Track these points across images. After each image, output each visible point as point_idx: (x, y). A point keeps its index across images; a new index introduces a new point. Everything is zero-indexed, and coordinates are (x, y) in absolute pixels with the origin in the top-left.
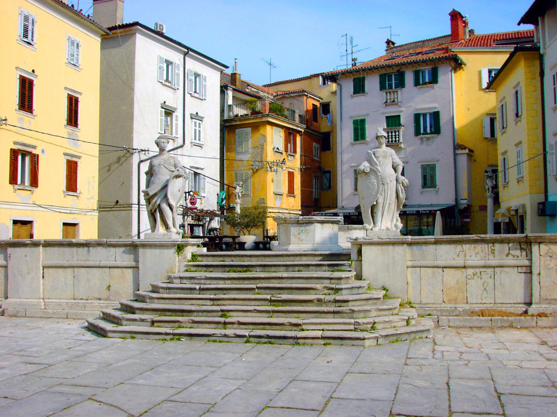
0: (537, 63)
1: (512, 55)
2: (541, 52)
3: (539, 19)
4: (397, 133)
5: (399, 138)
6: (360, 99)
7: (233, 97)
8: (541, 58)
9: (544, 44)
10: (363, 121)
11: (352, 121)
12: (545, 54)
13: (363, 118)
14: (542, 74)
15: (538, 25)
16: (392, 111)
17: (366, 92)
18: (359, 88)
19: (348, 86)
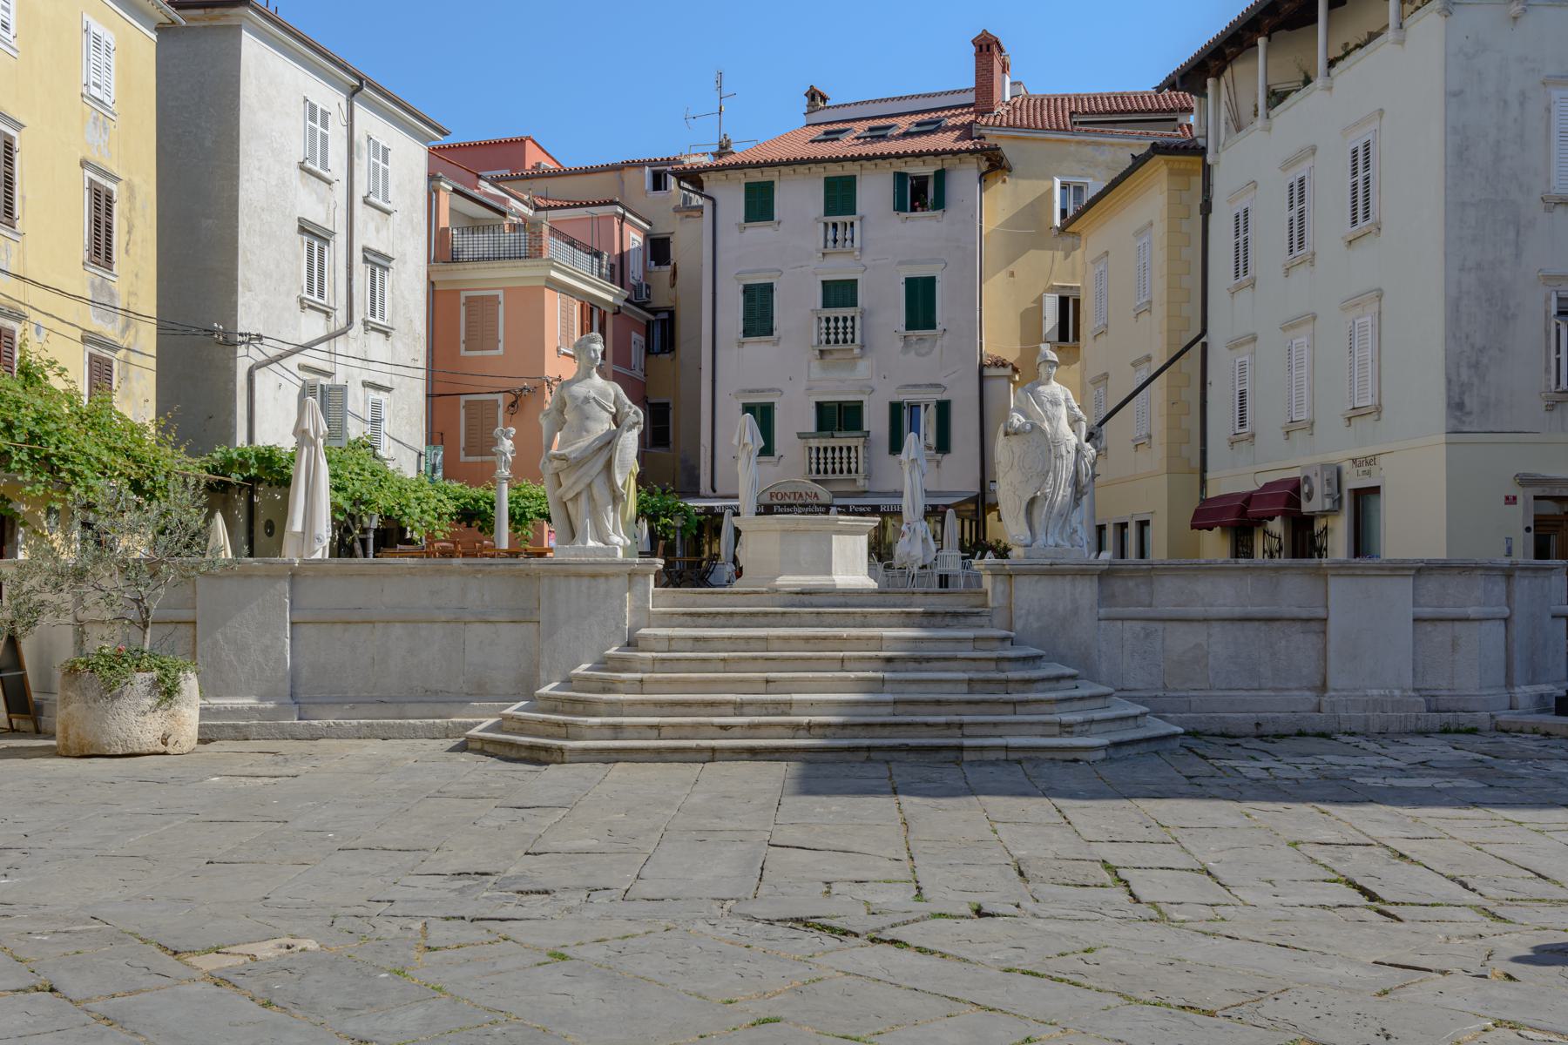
0: (1198, 181)
1: (1139, 162)
2: (1209, 160)
3: (1210, 81)
4: (849, 323)
5: (853, 333)
6: (760, 231)
7: (452, 210)
8: (1207, 171)
9: (1217, 143)
10: (769, 288)
11: (741, 288)
12: (1218, 163)
13: (768, 281)
14: (1206, 208)
15: (1206, 96)
16: (839, 268)
17: (776, 218)
18: (760, 204)
19: (732, 200)
